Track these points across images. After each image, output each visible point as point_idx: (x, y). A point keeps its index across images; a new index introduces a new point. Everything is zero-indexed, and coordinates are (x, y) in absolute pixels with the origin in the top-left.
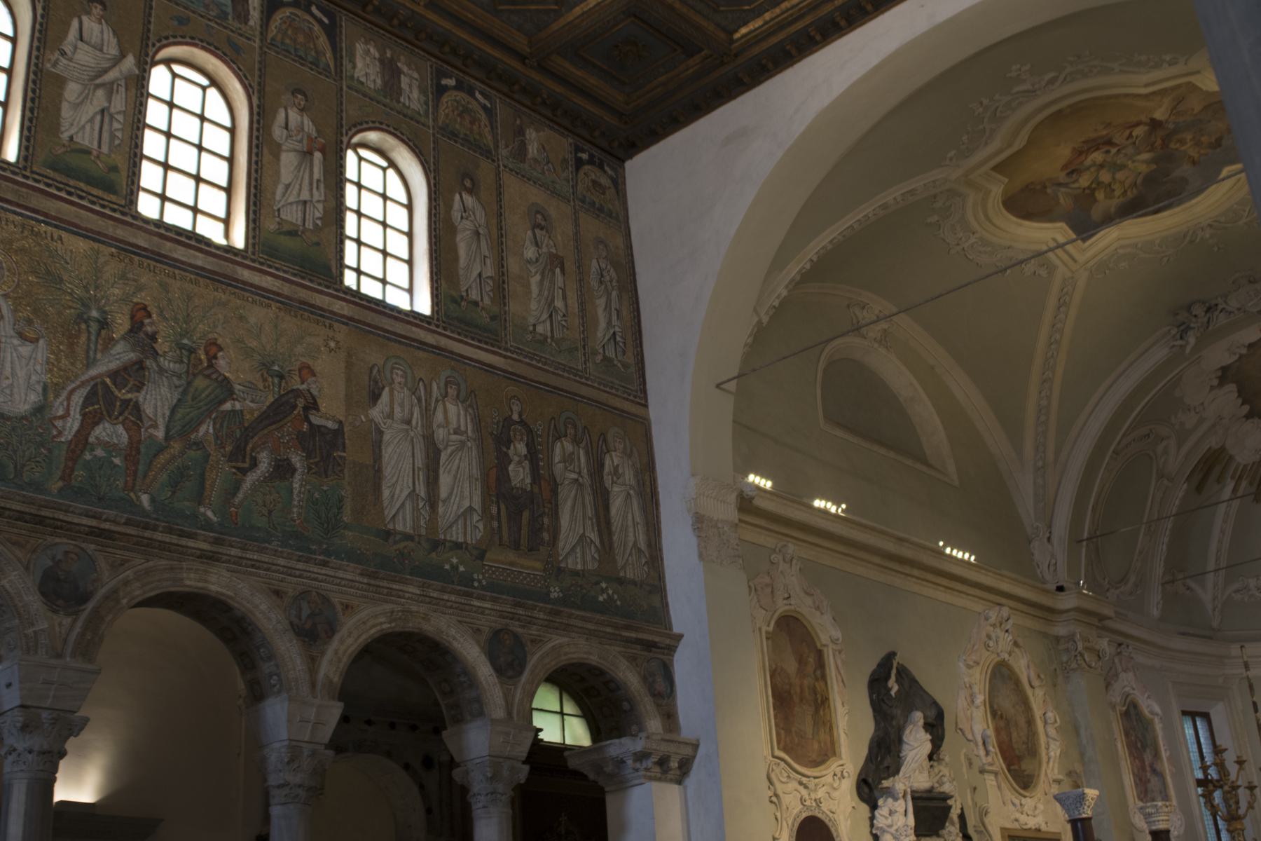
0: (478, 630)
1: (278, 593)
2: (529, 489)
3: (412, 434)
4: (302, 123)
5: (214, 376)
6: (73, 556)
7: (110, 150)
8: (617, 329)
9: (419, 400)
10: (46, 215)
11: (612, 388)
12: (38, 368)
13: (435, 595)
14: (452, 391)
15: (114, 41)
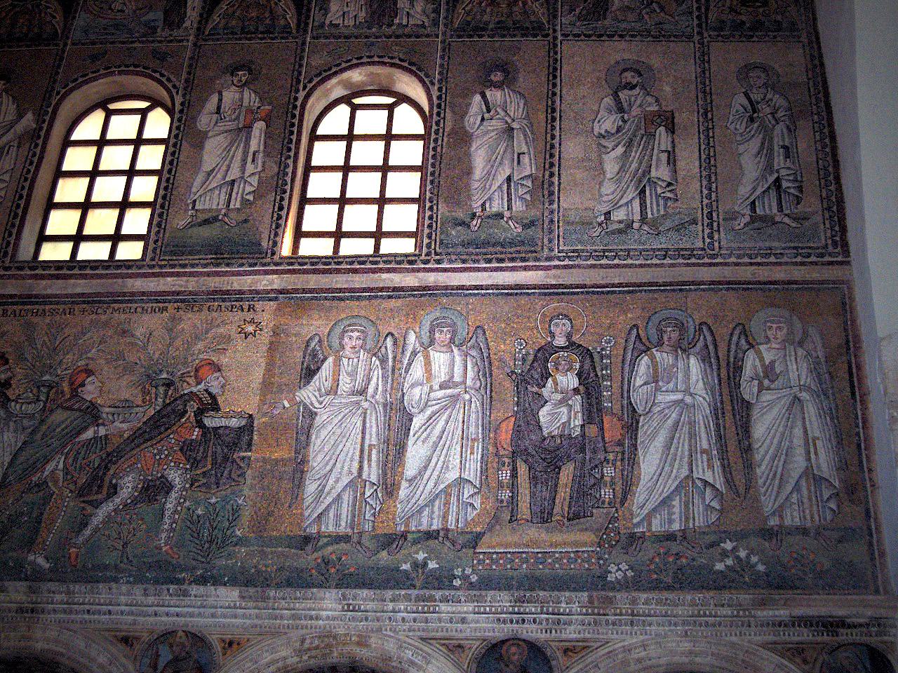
0: (460, 646)
1: (126, 640)
2: (578, 431)
3: (366, 405)
4: (241, 99)
5: (76, 406)
8: (783, 172)
9: (383, 361)
11: (767, 255)
14: (442, 336)
15: (12, 107)
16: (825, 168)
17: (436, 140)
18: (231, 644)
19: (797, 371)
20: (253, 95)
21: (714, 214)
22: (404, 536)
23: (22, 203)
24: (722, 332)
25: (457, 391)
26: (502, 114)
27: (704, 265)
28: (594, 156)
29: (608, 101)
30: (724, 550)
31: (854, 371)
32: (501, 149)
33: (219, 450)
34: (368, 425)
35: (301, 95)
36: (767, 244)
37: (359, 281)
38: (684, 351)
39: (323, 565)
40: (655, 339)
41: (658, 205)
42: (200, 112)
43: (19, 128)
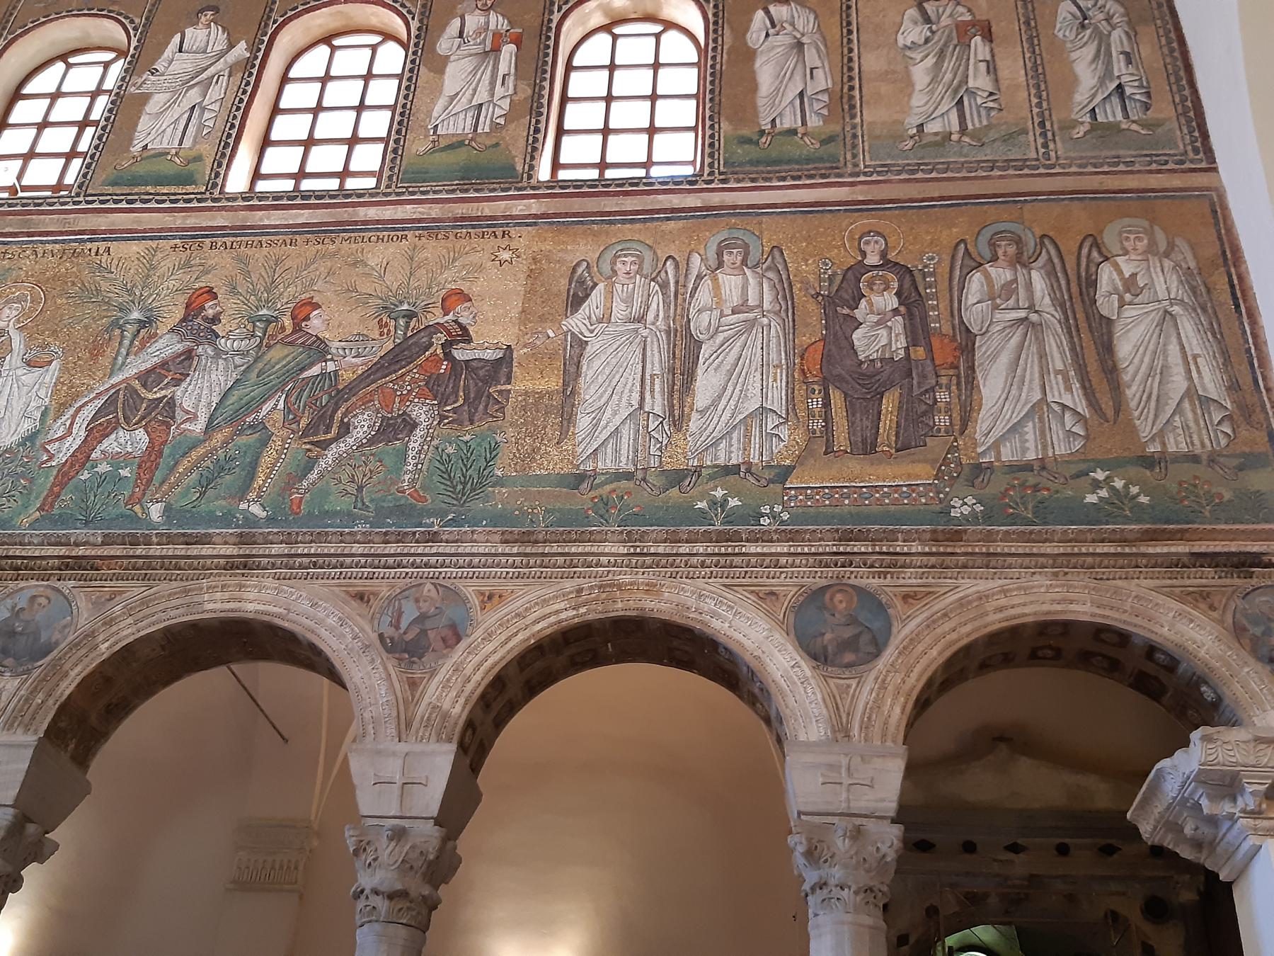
0: (772, 593)
1: (360, 597)
3: (645, 333)
4: (487, 23)
5: (300, 341)
6: (43, 601)
7: (195, 142)
8: (1124, 79)
9: (664, 286)
10: (94, 232)
11: (1117, 164)
12: (42, 393)
13: (660, 550)
15: (222, 37)
16: (1176, 73)
17: (714, 58)
18: (490, 597)
19: (1165, 283)
20: (500, 18)
21: (1048, 125)
22: (697, 471)
23: (234, 132)
24: (1069, 246)
25: (751, 315)
26: (789, 28)
27: (1040, 175)
28: (900, 68)
29: (912, 12)
30: (1095, 480)
31: (1236, 282)
32: (791, 63)
33: (472, 386)
34: (649, 353)
35: (556, 17)
36: (1113, 153)
37: (630, 204)
38: (1024, 266)
39: (601, 505)
40: (988, 255)
41: (979, 116)
42: (439, 37)
43: (232, 57)
